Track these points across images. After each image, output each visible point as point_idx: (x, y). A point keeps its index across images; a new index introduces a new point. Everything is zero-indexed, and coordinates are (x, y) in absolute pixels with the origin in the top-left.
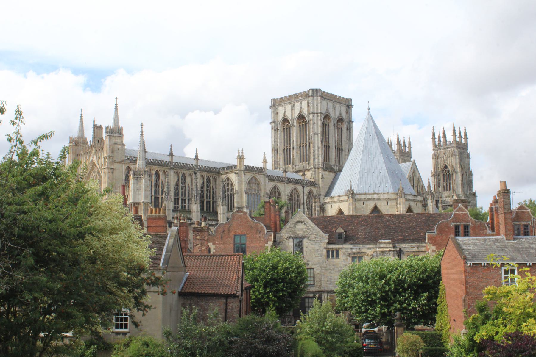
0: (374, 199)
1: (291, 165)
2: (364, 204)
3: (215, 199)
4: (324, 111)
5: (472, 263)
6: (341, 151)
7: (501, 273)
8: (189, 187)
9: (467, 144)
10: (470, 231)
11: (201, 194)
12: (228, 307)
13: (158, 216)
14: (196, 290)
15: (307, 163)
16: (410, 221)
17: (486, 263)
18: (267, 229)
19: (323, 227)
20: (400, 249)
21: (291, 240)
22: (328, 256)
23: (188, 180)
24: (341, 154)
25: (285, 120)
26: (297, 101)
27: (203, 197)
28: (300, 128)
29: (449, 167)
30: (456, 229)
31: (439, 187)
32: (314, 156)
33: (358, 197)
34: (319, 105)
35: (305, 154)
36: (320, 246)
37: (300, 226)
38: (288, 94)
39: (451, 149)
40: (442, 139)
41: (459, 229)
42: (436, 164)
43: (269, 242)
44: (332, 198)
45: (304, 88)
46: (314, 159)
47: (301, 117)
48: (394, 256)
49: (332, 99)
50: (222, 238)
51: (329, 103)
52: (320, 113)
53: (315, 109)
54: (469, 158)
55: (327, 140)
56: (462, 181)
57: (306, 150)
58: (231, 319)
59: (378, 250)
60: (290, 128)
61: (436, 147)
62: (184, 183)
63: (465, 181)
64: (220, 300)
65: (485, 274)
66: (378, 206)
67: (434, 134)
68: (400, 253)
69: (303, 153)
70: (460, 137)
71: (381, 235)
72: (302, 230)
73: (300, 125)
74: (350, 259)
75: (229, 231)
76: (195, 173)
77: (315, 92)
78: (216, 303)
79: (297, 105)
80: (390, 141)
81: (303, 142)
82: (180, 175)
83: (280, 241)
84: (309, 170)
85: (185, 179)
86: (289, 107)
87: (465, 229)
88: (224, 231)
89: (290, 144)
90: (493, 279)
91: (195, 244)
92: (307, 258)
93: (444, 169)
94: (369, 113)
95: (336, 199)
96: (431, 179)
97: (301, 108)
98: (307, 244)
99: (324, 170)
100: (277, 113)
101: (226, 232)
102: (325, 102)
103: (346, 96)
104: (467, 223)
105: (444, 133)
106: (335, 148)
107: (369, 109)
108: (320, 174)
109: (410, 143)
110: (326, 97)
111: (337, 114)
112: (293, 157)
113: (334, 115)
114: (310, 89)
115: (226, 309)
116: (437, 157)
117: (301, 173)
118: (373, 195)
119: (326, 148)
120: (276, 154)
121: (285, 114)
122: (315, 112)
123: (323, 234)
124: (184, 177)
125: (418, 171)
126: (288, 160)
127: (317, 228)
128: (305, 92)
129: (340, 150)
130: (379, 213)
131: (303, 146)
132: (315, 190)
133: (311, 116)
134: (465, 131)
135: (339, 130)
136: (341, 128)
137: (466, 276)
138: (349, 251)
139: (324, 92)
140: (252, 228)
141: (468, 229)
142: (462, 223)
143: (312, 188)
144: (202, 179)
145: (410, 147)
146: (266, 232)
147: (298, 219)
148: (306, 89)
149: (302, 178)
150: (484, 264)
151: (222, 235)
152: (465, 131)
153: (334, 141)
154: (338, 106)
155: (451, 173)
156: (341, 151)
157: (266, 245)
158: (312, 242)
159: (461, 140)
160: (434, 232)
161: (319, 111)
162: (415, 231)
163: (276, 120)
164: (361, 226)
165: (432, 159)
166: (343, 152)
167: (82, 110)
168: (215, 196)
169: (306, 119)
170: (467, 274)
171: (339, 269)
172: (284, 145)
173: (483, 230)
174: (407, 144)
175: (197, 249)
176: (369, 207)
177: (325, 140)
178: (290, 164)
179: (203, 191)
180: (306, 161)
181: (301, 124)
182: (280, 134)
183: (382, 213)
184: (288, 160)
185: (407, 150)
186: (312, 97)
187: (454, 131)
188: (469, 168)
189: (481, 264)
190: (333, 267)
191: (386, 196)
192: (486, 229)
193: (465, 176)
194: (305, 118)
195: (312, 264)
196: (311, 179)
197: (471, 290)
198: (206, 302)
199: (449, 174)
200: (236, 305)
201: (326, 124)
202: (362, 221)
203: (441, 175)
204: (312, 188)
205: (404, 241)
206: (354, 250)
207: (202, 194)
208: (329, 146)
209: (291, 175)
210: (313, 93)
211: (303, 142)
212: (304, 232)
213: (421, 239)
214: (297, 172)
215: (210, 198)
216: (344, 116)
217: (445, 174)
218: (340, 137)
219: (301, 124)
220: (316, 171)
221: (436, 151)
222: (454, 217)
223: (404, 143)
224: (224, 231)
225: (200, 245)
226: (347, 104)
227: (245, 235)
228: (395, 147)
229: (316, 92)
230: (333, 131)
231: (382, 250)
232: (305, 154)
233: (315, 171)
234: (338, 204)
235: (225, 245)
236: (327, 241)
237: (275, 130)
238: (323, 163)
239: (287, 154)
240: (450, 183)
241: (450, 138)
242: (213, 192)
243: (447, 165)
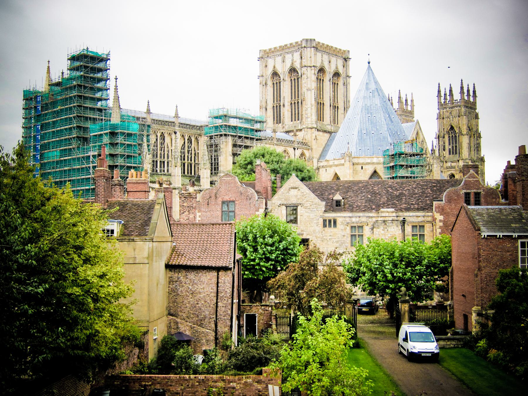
0: (373, 163)
1: (280, 124)
2: (362, 169)
3: (196, 162)
4: (318, 65)
5: (486, 234)
6: (336, 110)
7: (518, 246)
8: (168, 147)
9: (476, 103)
10: (482, 200)
11: (181, 156)
12: (220, 281)
13: (138, 180)
14: (183, 261)
15: (299, 122)
16: (415, 188)
17: (501, 234)
18: (258, 196)
19: (319, 194)
20: (404, 218)
21: (284, 207)
22: (325, 226)
23: (167, 140)
24: (336, 112)
25: (275, 74)
26: (288, 53)
27: (184, 160)
28: (292, 83)
29: (455, 128)
30: (466, 198)
31: (444, 150)
32: (306, 114)
33: (355, 161)
34: (313, 57)
35: (297, 112)
36: (315, 214)
37: (293, 192)
38: (277, 45)
39: (458, 108)
40: (448, 98)
41: (469, 198)
42: (440, 125)
43: (260, 210)
44: (327, 161)
45: (297, 38)
46: (307, 118)
47: (293, 70)
48: (397, 226)
49: (328, 51)
50: (208, 205)
51: (324, 55)
52: (314, 66)
53: (309, 62)
54: (478, 119)
55: (321, 97)
56: (470, 144)
57: (298, 108)
58: (222, 294)
59: (379, 219)
60: (280, 82)
61: (441, 106)
62: (162, 144)
63: (472, 145)
64: (211, 273)
65: (500, 246)
66: (378, 171)
67: (439, 92)
68: (404, 223)
69: (295, 111)
70: (468, 95)
71: (384, 203)
72: (296, 196)
73: (291, 80)
74: (349, 228)
75: (216, 197)
76: (175, 133)
77: (309, 43)
78: (206, 276)
79: (289, 57)
80: (390, 99)
81: (295, 98)
82: (159, 135)
83: (272, 209)
84: (301, 130)
85: (164, 139)
86: (279, 59)
87: (476, 198)
88: (210, 197)
89: (280, 101)
90: (509, 252)
91: (182, 212)
92: (302, 227)
93: (449, 130)
94: (369, 67)
95: (331, 163)
96: (435, 142)
97: (292, 60)
98: (302, 212)
99: (318, 130)
100: (266, 66)
101: (213, 197)
102: (319, 55)
103: (343, 48)
104: (479, 191)
105: (451, 91)
106: (330, 106)
107: (369, 63)
108: (314, 135)
109: (412, 101)
110: (322, 49)
112: (284, 115)
113: (330, 70)
114: (303, 40)
115: (218, 283)
116: (442, 117)
117: (292, 134)
118: (372, 159)
119: (320, 105)
121: (274, 67)
122: (309, 65)
123: (320, 201)
124: (163, 136)
125: (422, 132)
126: (278, 119)
127: (313, 195)
128: (296, 43)
129: (335, 108)
130: (379, 178)
131: (295, 103)
132: (307, 153)
133: (304, 69)
134: (474, 87)
135: (335, 85)
136: (337, 84)
137: (479, 249)
138: (348, 220)
139: (319, 43)
140: (241, 194)
141: (479, 198)
142: (473, 191)
143: (304, 150)
144: (182, 139)
145: (412, 106)
146: (257, 198)
147: (292, 185)
148: (299, 40)
149: (293, 139)
150: (500, 236)
151: (208, 202)
152: (474, 87)
153: (329, 98)
154: (333, 60)
155: (457, 135)
156: (336, 110)
157: (257, 213)
158: (307, 210)
159: (469, 98)
160: (442, 201)
161: (312, 65)
162: (420, 199)
163: (264, 75)
164: (362, 193)
165: (437, 119)
166: (339, 110)
167: (49, 62)
168: (196, 158)
169: (298, 73)
170: (481, 247)
171: (337, 239)
172: (274, 102)
173: (496, 199)
174: (409, 102)
175: (184, 217)
176: (368, 171)
177: (319, 97)
178: (280, 123)
179: (184, 153)
180: (298, 120)
181: (293, 79)
182: (270, 89)
183: (381, 179)
184: (278, 119)
185: (409, 108)
186: (305, 49)
187: (462, 88)
188: (477, 130)
189: (497, 235)
190: (330, 237)
192: (499, 198)
193: (472, 138)
194: (297, 71)
195: (307, 234)
196: (303, 140)
197: (484, 264)
198: (196, 276)
199: (456, 136)
200: (229, 279)
201: (320, 79)
202: (362, 187)
203: (447, 137)
204: (304, 150)
205: (408, 210)
206: (354, 220)
207: (183, 156)
208: (323, 103)
209: (281, 135)
210: (307, 44)
211: (295, 98)
212: (298, 199)
213: (428, 208)
214: (287, 132)
215: (191, 161)
216: (341, 70)
217: (451, 136)
218: (336, 93)
219: (293, 79)
220: (309, 132)
221: (442, 111)
222: (465, 184)
223: (406, 100)
224: (210, 197)
225: (187, 213)
226: (344, 56)
227: (233, 202)
228: (396, 106)
230: (327, 86)
231: (382, 219)
232: (297, 112)
233: (307, 131)
234: (334, 168)
235: (212, 213)
236: (324, 209)
238: (316, 123)
239: (277, 112)
240: (456, 146)
241: (457, 96)
242: (195, 154)
243: (453, 125)
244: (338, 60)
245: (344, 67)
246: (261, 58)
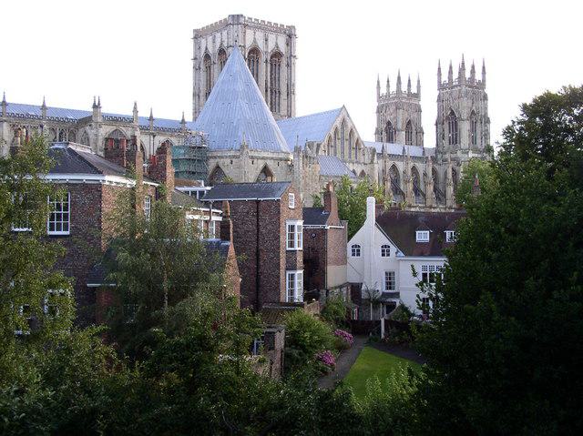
9: (484, 80)
25: (207, 57)
47: (222, 52)
79: (218, 35)
102: (249, 33)
103: (287, 22)
111: (271, 46)
120: (197, 100)
121: (206, 49)
133: (230, 49)
145: (419, 87)
154: (272, 37)
185: (414, 90)
188: (486, 114)
191: (232, 153)
216: (283, 48)
229: (236, 19)
237: (197, 69)
244: (279, 38)
245: (287, 44)
246: (195, 38)
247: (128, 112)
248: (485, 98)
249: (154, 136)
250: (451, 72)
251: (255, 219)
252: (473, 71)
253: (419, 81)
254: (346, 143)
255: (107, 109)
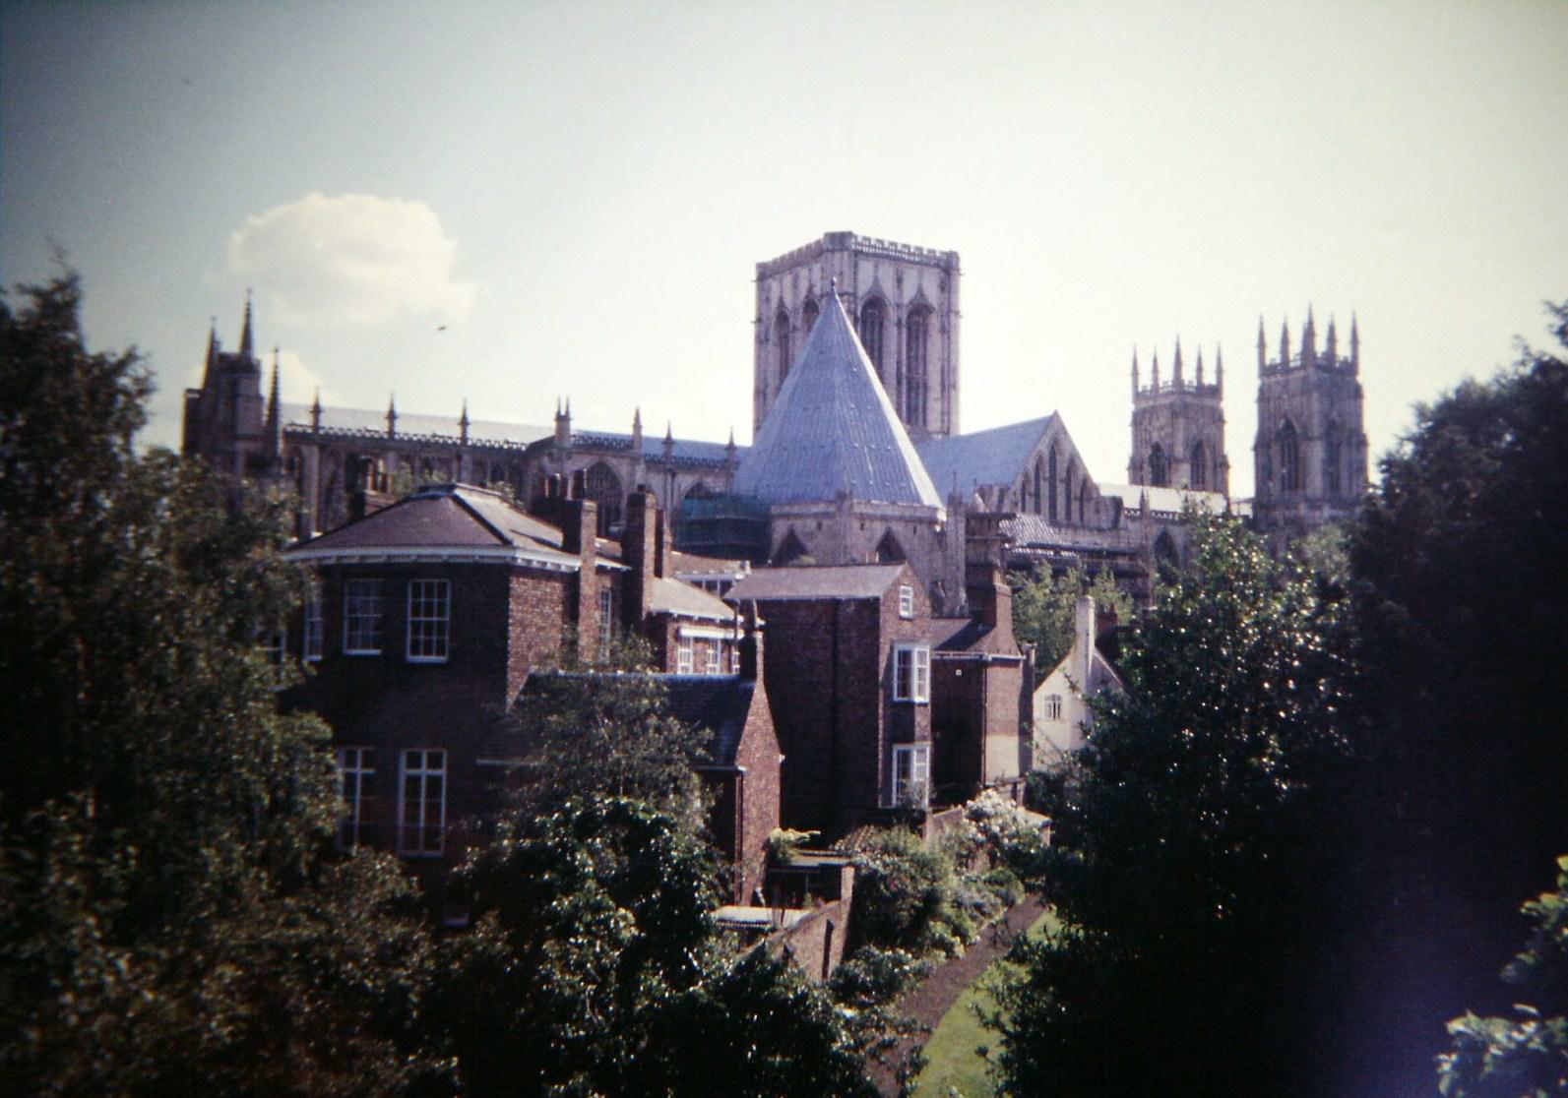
9: (1355, 357)
25: (782, 317)
47: (810, 307)
111: (909, 293)
120: (761, 401)
145: (1219, 371)
185: (1209, 379)
191: (821, 508)
216: (933, 296)
229: (839, 241)
237: (761, 341)
247: (625, 429)
248: (1357, 393)
249: (674, 475)
250: (1285, 342)
251: (829, 637)
252: (1332, 339)
253: (1219, 360)
254: (1061, 489)
255: (578, 425)
